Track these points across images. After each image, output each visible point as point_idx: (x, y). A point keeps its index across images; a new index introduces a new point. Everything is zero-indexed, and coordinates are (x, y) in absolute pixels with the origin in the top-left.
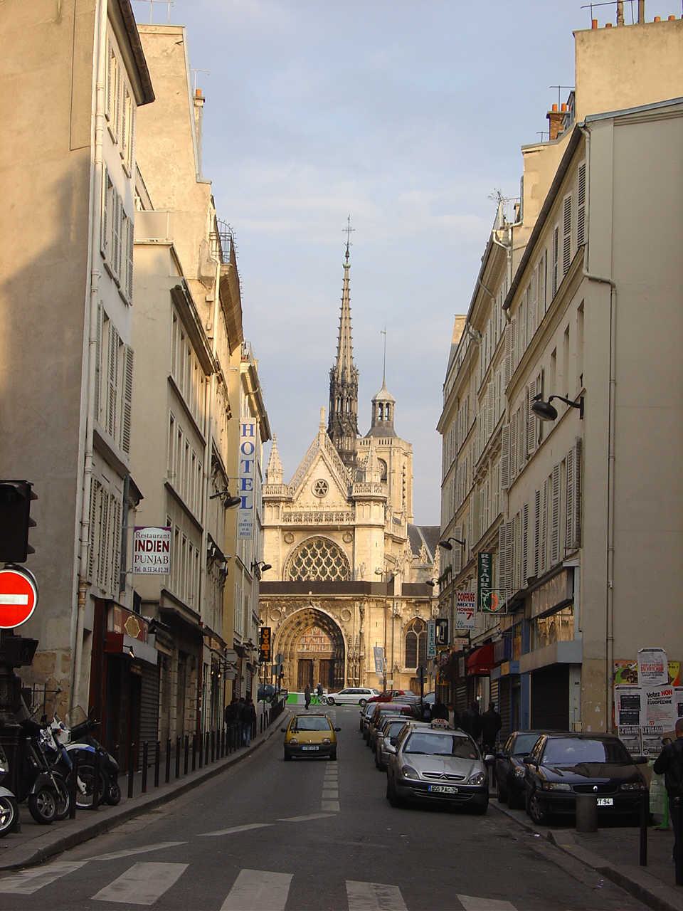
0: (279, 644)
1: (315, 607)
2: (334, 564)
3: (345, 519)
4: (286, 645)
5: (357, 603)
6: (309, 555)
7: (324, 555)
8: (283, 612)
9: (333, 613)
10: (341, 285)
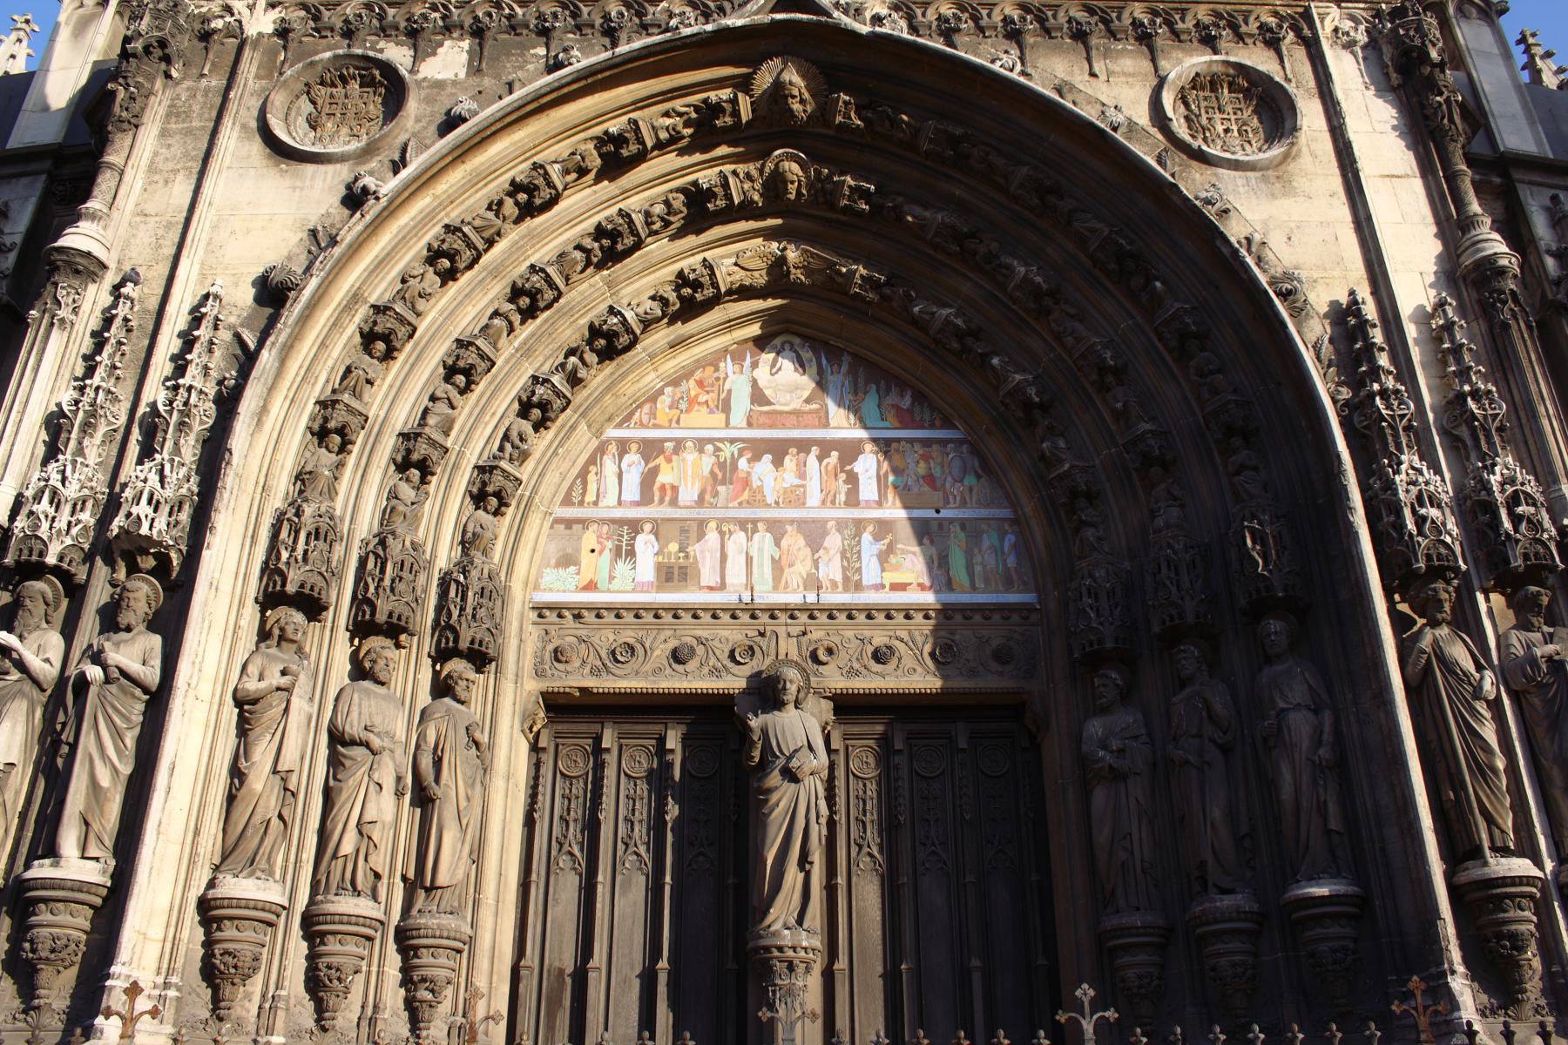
8: (439, 85)
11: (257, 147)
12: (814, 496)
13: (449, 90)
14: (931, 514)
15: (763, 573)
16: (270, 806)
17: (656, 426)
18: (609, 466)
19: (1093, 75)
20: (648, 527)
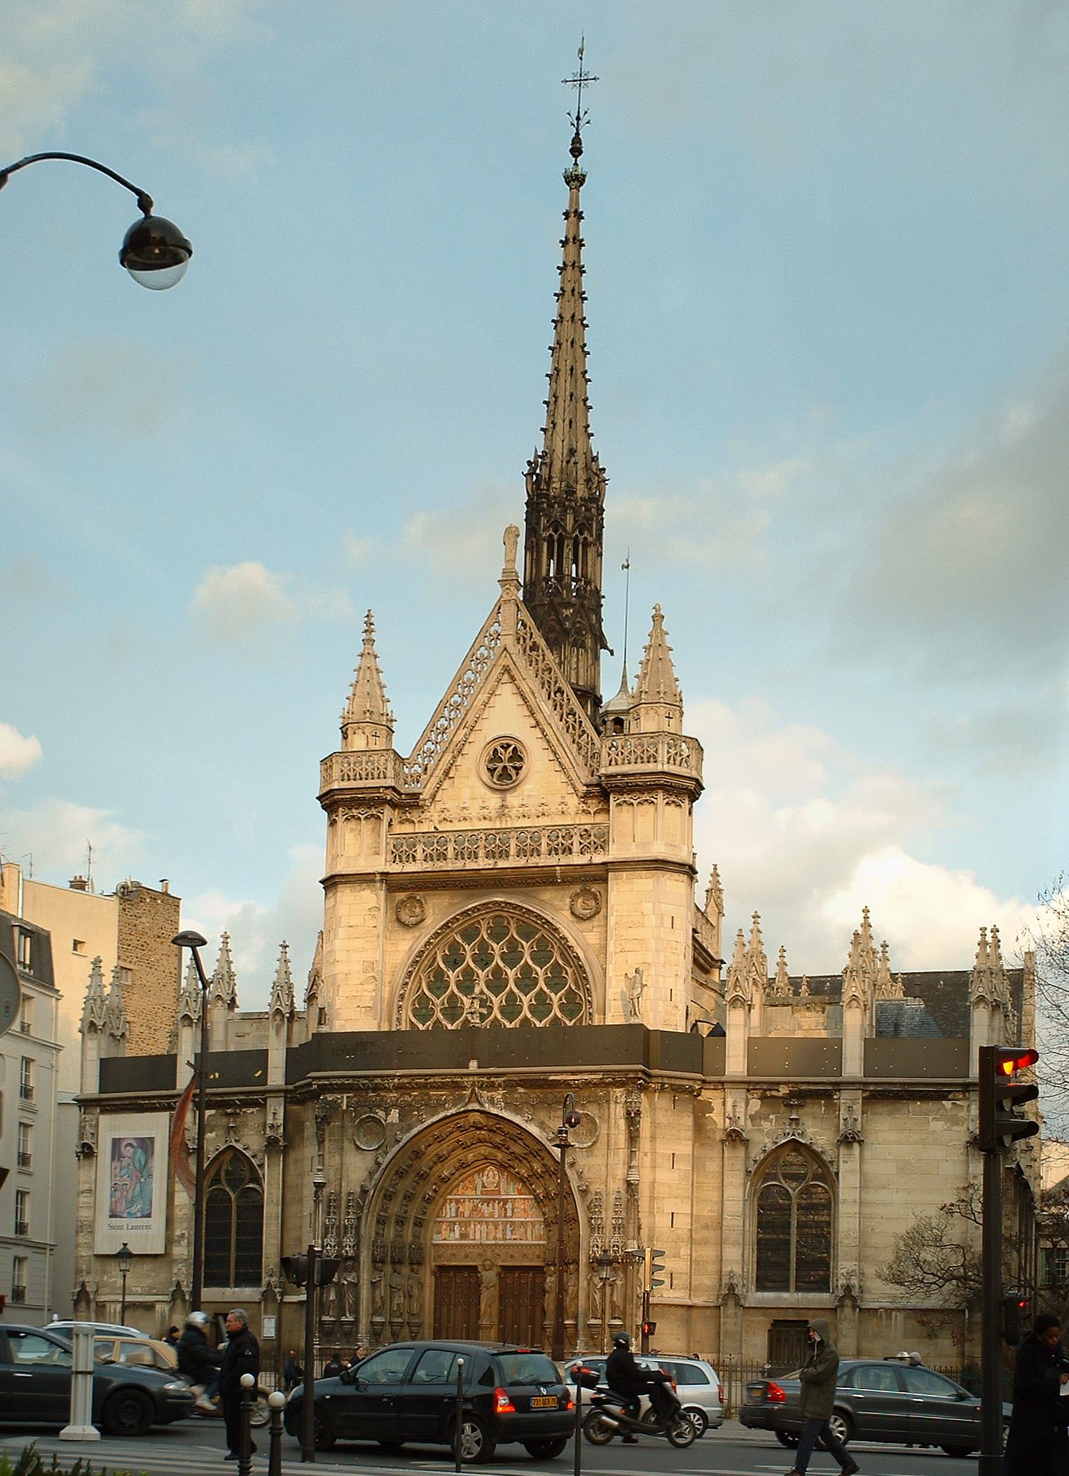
0: (381, 1221)
1: (487, 1107)
2: (541, 984)
3: (576, 848)
4: (401, 1222)
5: (619, 1092)
6: (469, 960)
7: (512, 957)
8: (392, 1124)
9: (542, 1125)
10: (561, 229)
11: (353, 1146)
14: (523, 1220)
16: (379, 1304)
18: (448, 1207)
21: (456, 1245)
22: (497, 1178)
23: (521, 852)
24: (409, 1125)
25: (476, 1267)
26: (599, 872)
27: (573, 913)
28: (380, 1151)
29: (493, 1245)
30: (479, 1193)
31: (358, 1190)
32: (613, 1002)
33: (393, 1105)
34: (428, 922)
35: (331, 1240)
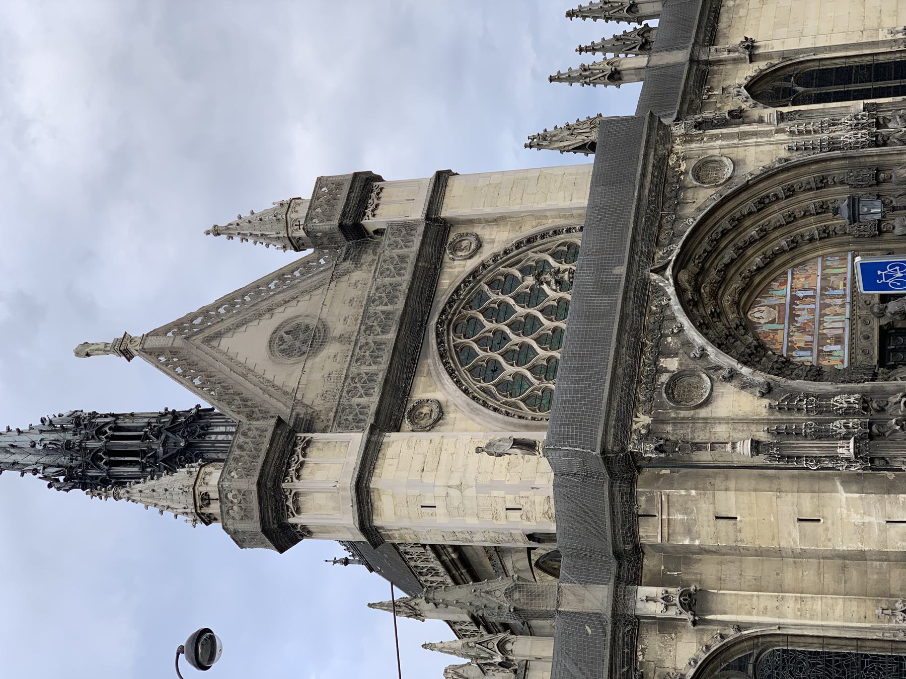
7: (500, 312)
8: (680, 364)
12: (813, 306)
13: (683, 361)
14: (819, 278)
15: (837, 318)
17: (782, 348)
18: (798, 359)
19: (694, 202)
20: (821, 348)
21: (851, 348)
22: (763, 308)
23: (392, 300)
24: (683, 345)
25: (881, 327)
26: (434, 229)
27: (470, 258)
28: (715, 377)
29: (852, 307)
30: (781, 327)
31: (766, 402)
32: (574, 201)
33: (655, 364)
34: (439, 396)
35: (838, 425)
